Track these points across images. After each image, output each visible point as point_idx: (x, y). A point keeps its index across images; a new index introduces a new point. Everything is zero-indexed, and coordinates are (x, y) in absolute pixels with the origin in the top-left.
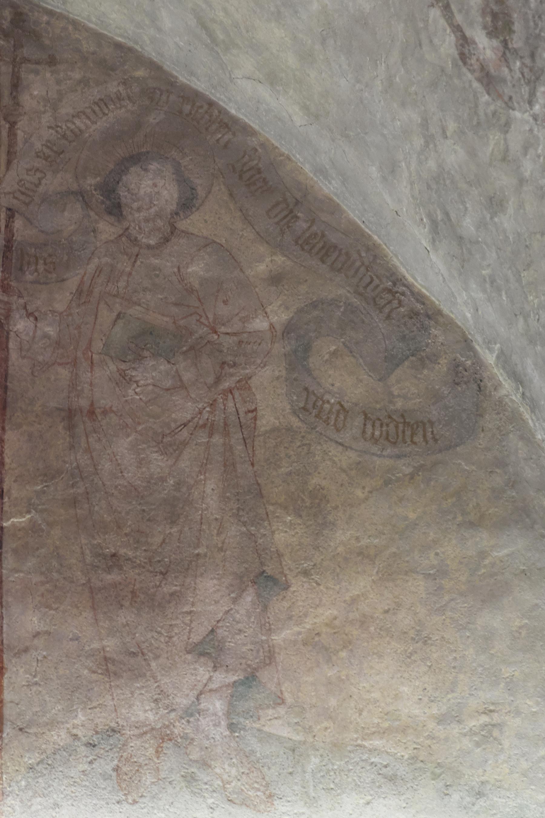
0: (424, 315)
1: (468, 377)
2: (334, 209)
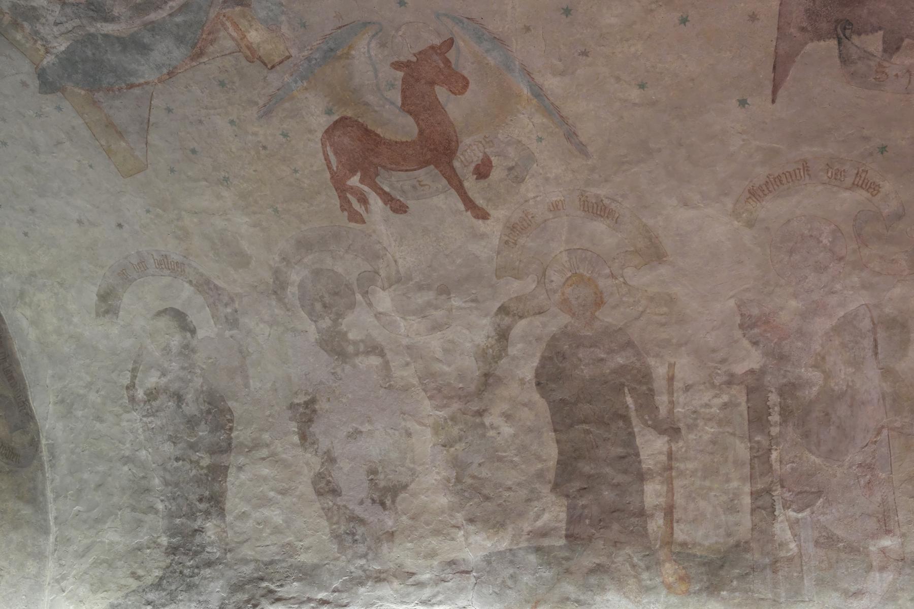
0: (28, 416)
1: (34, 444)
2: (18, 364)
